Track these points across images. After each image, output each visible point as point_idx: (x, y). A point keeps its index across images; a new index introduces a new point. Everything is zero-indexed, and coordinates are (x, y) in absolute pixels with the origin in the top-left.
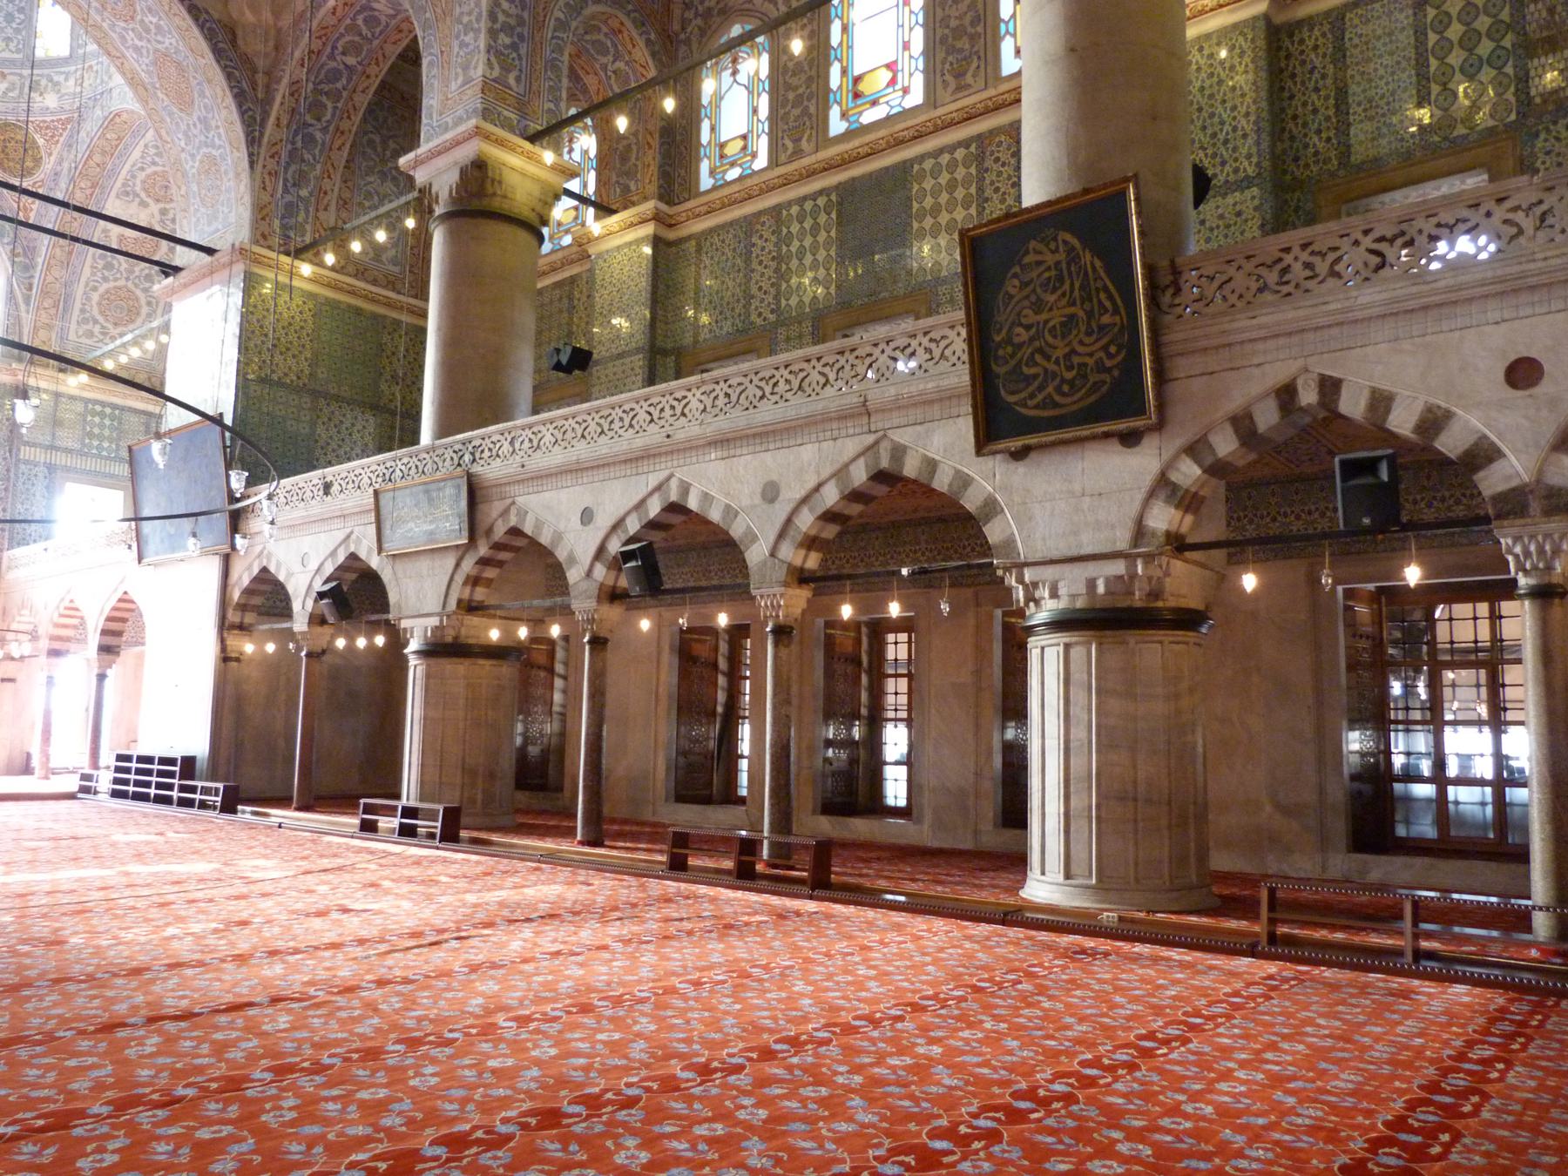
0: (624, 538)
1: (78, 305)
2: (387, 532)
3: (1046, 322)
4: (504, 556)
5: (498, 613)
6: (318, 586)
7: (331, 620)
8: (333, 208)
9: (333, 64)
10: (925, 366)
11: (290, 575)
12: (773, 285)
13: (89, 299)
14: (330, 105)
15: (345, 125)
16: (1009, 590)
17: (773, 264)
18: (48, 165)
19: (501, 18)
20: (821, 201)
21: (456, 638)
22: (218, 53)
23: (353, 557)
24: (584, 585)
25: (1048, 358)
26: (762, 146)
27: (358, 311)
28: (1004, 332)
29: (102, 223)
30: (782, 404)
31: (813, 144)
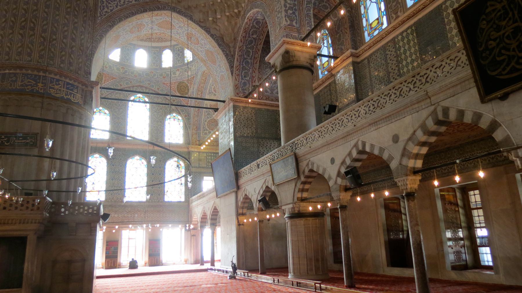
0: (345, 166)
1: (202, 127)
2: (275, 177)
3: (504, 34)
4: (310, 180)
5: (312, 200)
6: (259, 198)
7: (264, 209)
8: (257, 81)
9: (250, 39)
10: (450, 71)
11: (252, 196)
12: (396, 66)
13: (205, 124)
14: (251, 51)
15: (256, 56)
16: (513, 162)
17: (395, 59)
18: (190, 91)
19: (288, 6)
20: (409, 31)
21: (299, 211)
22: (219, 45)
23: (267, 187)
24: (335, 187)
25: (509, 50)
26: (385, 19)
27: (268, 110)
28: (483, 46)
29: (205, 101)
30: (394, 103)
31: (402, 12)
